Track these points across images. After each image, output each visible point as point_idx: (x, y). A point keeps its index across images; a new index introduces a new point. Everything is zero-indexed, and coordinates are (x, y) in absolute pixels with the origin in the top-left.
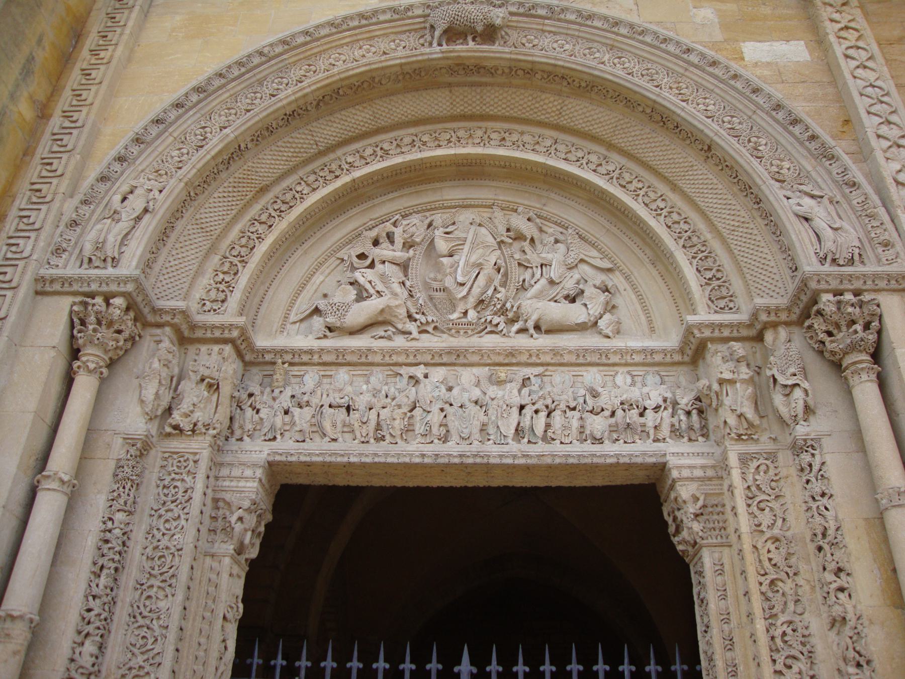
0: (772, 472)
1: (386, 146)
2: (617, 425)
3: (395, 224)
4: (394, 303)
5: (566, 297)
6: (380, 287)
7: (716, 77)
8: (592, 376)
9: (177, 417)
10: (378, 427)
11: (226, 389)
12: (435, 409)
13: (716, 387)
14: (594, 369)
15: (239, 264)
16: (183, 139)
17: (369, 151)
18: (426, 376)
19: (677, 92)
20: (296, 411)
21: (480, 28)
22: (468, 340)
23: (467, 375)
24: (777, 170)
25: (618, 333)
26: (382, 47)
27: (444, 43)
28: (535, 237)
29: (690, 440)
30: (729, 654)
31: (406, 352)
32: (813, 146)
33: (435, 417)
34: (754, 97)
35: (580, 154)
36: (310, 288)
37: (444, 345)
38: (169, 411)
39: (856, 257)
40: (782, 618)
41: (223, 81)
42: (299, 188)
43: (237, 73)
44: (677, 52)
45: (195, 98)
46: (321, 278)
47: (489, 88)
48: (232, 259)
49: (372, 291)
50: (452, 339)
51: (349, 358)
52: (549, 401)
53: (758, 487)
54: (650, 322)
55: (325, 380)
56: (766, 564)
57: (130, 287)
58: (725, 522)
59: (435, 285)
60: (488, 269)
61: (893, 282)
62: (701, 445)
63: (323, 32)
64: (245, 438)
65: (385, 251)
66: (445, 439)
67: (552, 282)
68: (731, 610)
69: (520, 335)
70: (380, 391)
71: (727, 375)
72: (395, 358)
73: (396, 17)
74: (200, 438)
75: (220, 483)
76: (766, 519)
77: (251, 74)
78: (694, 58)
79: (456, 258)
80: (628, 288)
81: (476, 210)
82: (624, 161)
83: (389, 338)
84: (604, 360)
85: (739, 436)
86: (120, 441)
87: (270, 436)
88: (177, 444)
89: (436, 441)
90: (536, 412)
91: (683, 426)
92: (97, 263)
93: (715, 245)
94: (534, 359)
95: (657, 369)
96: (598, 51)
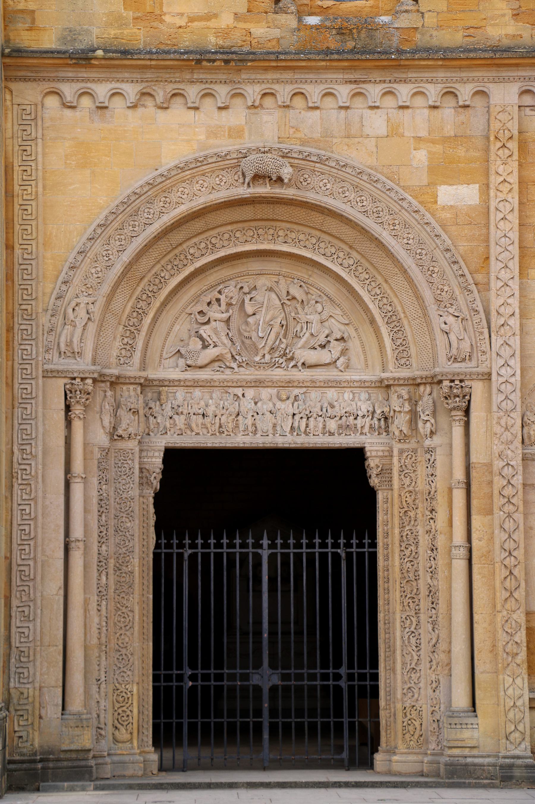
0: (413, 459)
1: (214, 241)
2: (341, 425)
3: (220, 292)
4: (224, 351)
5: (320, 346)
6: (215, 339)
7: (417, 220)
8: (331, 394)
9: (120, 432)
10: (220, 426)
11: (141, 412)
12: (249, 416)
13: (392, 413)
14: (333, 389)
15: (135, 332)
16: (95, 259)
17: (203, 245)
18: (243, 395)
19: (392, 228)
20: (176, 417)
21: (274, 179)
22: (265, 373)
23: (265, 393)
24: (440, 293)
25: (347, 367)
26: (211, 182)
27: (251, 185)
28: (304, 300)
30: (385, 540)
32: (461, 280)
34: (436, 239)
36: (172, 335)
37: (252, 377)
39: (467, 358)
40: (407, 528)
41: (114, 216)
42: (162, 275)
43: (122, 209)
44: (396, 199)
45: (99, 231)
46: (178, 327)
47: (278, 205)
48: (130, 328)
49: (211, 342)
50: (256, 372)
51: (200, 384)
52: (308, 412)
53: (406, 466)
54: (366, 361)
56: (404, 503)
57: (96, 375)
58: (391, 478)
59: (246, 334)
60: (276, 328)
61: (480, 376)
63: (173, 173)
64: (151, 433)
65: (215, 313)
66: (255, 433)
67: (312, 334)
68: (389, 520)
69: (295, 369)
70: (219, 404)
71: (397, 409)
72: (226, 384)
73: (220, 159)
74: (133, 441)
75: (142, 460)
76: (407, 481)
77: (130, 208)
78: (405, 205)
79: (257, 316)
80: (356, 337)
81: (268, 276)
82: (359, 257)
83: (222, 372)
84: (338, 385)
85: (400, 440)
86: (97, 449)
87: (164, 432)
88: (121, 445)
89: (250, 434)
90: (301, 418)
91: (376, 427)
93: (405, 322)
94: (301, 384)
95: (367, 389)
96: (348, 190)
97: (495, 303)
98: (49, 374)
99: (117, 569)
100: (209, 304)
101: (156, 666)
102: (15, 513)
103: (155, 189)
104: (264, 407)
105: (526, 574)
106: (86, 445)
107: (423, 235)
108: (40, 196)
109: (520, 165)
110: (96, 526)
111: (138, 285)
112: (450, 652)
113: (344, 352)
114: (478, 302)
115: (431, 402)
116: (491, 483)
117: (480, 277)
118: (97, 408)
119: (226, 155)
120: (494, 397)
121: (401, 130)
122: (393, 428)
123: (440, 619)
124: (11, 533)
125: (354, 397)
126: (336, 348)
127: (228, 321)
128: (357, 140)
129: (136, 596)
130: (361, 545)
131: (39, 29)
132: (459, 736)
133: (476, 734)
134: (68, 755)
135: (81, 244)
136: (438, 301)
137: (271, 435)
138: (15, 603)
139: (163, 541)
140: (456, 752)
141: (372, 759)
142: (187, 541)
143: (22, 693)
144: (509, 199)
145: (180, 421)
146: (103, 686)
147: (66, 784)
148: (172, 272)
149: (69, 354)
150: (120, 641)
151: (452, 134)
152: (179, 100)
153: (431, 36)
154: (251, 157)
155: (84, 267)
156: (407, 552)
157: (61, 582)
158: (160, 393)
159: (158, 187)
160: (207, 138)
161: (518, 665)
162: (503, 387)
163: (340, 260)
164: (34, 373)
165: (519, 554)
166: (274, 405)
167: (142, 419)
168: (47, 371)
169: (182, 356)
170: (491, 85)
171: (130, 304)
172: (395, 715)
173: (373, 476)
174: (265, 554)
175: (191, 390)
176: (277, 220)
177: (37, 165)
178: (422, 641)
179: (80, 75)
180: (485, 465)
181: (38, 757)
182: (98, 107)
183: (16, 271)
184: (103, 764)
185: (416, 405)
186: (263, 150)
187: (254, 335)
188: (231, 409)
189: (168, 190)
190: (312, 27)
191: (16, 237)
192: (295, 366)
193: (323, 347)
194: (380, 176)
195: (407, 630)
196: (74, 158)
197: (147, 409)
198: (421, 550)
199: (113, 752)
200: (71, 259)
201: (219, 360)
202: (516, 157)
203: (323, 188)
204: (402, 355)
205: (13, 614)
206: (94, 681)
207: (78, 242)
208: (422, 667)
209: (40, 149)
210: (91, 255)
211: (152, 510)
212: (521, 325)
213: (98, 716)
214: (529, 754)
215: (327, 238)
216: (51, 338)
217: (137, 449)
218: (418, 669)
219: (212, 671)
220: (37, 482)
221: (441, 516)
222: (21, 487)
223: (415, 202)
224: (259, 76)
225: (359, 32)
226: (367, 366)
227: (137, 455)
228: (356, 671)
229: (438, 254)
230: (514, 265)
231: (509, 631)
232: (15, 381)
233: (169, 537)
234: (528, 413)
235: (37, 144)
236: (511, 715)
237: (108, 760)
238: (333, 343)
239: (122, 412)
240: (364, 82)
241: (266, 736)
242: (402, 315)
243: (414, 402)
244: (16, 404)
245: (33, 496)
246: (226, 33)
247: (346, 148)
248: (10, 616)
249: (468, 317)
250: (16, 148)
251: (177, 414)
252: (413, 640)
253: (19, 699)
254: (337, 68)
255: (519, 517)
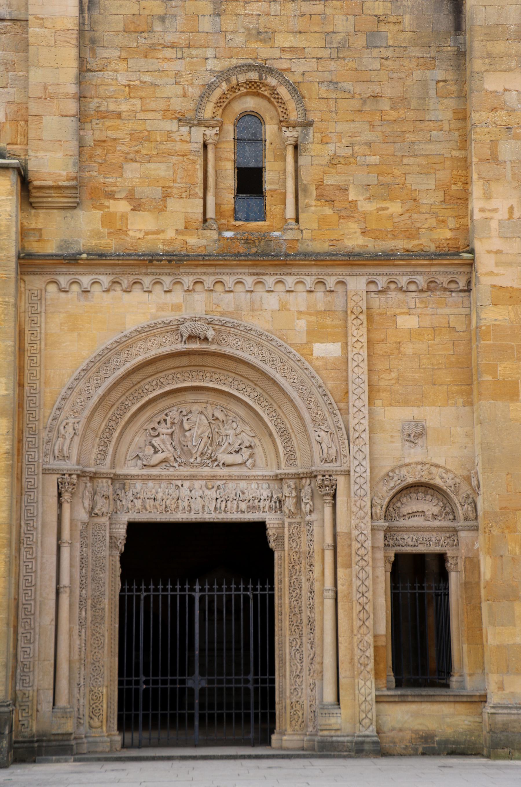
1: (162, 380)
3: (166, 415)
4: (169, 455)
5: (235, 451)
6: (163, 447)
8: (243, 484)
9: (96, 511)
10: (166, 507)
11: (111, 497)
12: (186, 500)
14: (244, 481)
17: (154, 383)
18: (182, 485)
20: (135, 501)
23: (197, 484)
25: (254, 466)
29: (275, 512)
31: (174, 476)
32: (330, 407)
33: (186, 503)
34: (312, 379)
35: (244, 387)
37: (188, 473)
38: (92, 509)
40: (294, 577)
41: (93, 364)
43: (98, 359)
45: (82, 374)
48: (103, 439)
49: (160, 449)
50: (191, 470)
51: (153, 478)
52: (226, 497)
54: (267, 462)
55: (144, 485)
56: (292, 560)
57: (79, 472)
59: (184, 444)
60: (205, 439)
62: (278, 515)
63: (133, 335)
65: (163, 429)
66: (190, 511)
67: (229, 444)
69: (217, 468)
71: (287, 495)
72: (170, 478)
76: (294, 545)
78: (291, 356)
79: (192, 431)
82: (261, 391)
88: (97, 520)
92: (60, 458)
93: (293, 435)
97: (352, 423)
98: (46, 472)
99: (93, 606)
100: (159, 423)
101: (121, 674)
102: (21, 568)
103: (121, 345)
104: (197, 493)
105: (374, 609)
106: (72, 520)
107: (304, 376)
108: (43, 352)
109: (368, 330)
110: (78, 577)
111: (110, 410)
112: (322, 663)
113: (251, 456)
114: (341, 422)
115: (310, 490)
116: (350, 546)
117: (342, 405)
118: (80, 495)
119: (169, 323)
120: (352, 486)
121: (288, 307)
122: (285, 508)
123: (316, 640)
124: (19, 582)
125: (258, 487)
126: (246, 453)
127: (172, 434)
128: (258, 313)
129: (106, 625)
130: (263, 589)
131: (44, 241)
132: (328, 722)
133: (339, 721)
134: (56, 738)
135: (70, 382)
136: (314, 421)
137: (201, 513)
138: (21, 630)
139: (127, 587)
140: (326, 733)
141: (270, 738)
142: (143, 587)
143: (25, 694)
144: (361, 353)
145: (138, 503)
146: (82, 688)
147: (54, 758)
148: (133, 401)
149: (60, 458)
150: (94, 658)
151: (323, 309)
152: (138, 286)
153: (308, 245)
154: (187, 324)
155: (72, 398)
156: (294, 594)
157: (53, 615)
158: (124, 484)
159: (123, 344)
160: (157, 311)
161: (368, 672)
162: (358, 480)
163: (248, 393)
164: (36, 471)
165: (369, 595)
166: (203, 492)
167: (112, 502)
168: (45, 469)
169: (140, 458)
170: (348, 278)
171: (104, 423)
172: (285, 707)
173: (271, 541)
174: (197, 595)
175: (146, 482)
176: (205, 366)
177: (41, 330)
178: (304, 656)
179: (71, 270)
180: (346, 533)
181: (35, 739)
182: (83, 291)
183: (25, 401)
184: (81, 743)
185: (300, 492)
186: (194, 319)
187: (189, 444)
188: (174, 495)
189: (130, 346)
190: (228, 239)
191: (25, 379)
192: (218, 465)
193: (237, 452)
194: (274, 337)
195: (294, 648)
196: (66, 325)
197: (115, 495)
198: (303, 592)
199: (88, 735)
200: (63, 393)
201: (166, 461)
202: (365, 325)
203: (236, 345)
204: (290, 458)
205: (19, 638)
206: (76, 685)
207: (68, 381)
208: (303, 674)
209: (43, 319)
210: (77, 390)
211: (118, 565)
212: (370, 438)
213: (79, 710)
214: (375, 734)
215: (240, 378)
216: (48, 447)
217: (108, 523)
218: (301, 675)
219: (160, 678)
220: (37, 546)
221: (317, 569)
222: (26, 550)
223: (298, 355)
224: (191, 271)
225: (259, 242)
226: (267, 465)
227: (108, 528)
228: (259, 677)
229: (314, 390)
230: (365, 397)
231: (362, 648)
232: (23, 476)
233: (130, 584)
234: (375, 498)
235: (41, 316)
236: (363, 707)
237: (85, 740)
238: (244, 449)
239: (97, 498)
240: (263, 275)
241: (197, 723)
242: (291, 431)
243: (298, 490)
244: (24, 492)
245: (34, 556)
246: (170, 242)
247: (251, 318)
248: (17, 640)
249: (334, 432)
250: (27, 319)
251: (136, 498)
252: (298, 656)
253: (22, 698)
254: (245, 266)
255: (369, 569)
